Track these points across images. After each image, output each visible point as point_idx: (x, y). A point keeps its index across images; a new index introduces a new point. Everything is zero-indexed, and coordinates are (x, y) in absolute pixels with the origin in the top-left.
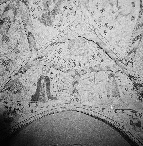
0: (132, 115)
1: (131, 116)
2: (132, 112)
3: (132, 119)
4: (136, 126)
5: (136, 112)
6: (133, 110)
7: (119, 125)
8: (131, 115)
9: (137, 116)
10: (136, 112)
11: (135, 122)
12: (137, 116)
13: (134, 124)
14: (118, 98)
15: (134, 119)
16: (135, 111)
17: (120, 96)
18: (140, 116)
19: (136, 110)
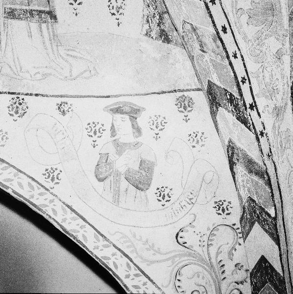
0: (113, 127)
1: (108, 133)
2: (118, 110)
3: (111, 150)
4: (124, 184)
5: (134, 113)
6: (121, 99)
7: (25, 181)
8: (108, 127)
9: (138, 130)
10: (134, 113)
11: (124, 163)
12: (138, 130)
13: (118, 174)
14: (44, 26)
15: (120, 148)
16: (125, 104)
17: (52, 15)
18: (157, 131)
19: (137, 102)
